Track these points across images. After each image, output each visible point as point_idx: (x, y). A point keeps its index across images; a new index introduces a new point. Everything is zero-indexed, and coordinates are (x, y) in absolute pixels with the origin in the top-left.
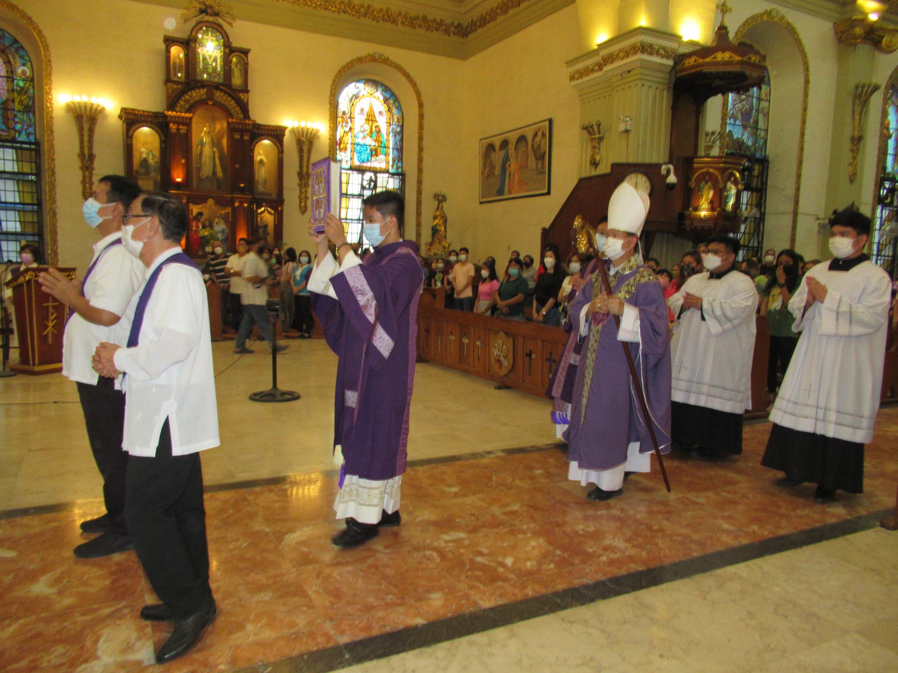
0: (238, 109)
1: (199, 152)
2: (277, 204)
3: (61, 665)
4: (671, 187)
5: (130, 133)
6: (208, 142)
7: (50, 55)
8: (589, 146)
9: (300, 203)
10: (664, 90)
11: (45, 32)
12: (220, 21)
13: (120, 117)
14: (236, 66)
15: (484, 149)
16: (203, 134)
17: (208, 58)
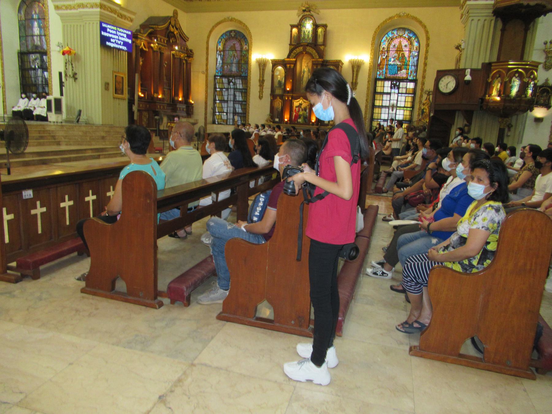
0: (316, 54)
4: (468, 82)
6: (306, 71)
10: (491, 20)
11: (251, 31)
12: (312, 13)
17: (306, 32)
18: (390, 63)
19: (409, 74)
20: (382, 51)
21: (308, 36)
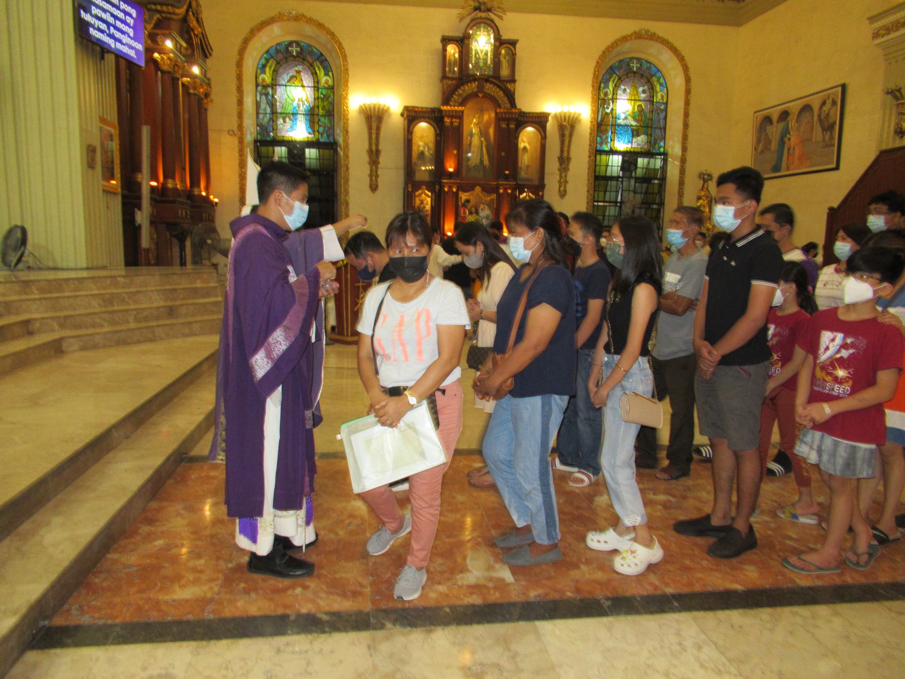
1: (468, 142)
2: (539, 187)
3: (443, 572)
5: (410, 129)
6: (476, 132)
7: (347, 65)
8: (894, 112)
9: (560, 187)
11: (345, 45)
12: (492, 16)
13: (402, 115)
14: (505, 58)
15: (758, 123)
16: (472, 126)
17: (479, 52)
18: (619, 122)
19: (652, 142)
20: (604, 100)
21: (485, 60)
